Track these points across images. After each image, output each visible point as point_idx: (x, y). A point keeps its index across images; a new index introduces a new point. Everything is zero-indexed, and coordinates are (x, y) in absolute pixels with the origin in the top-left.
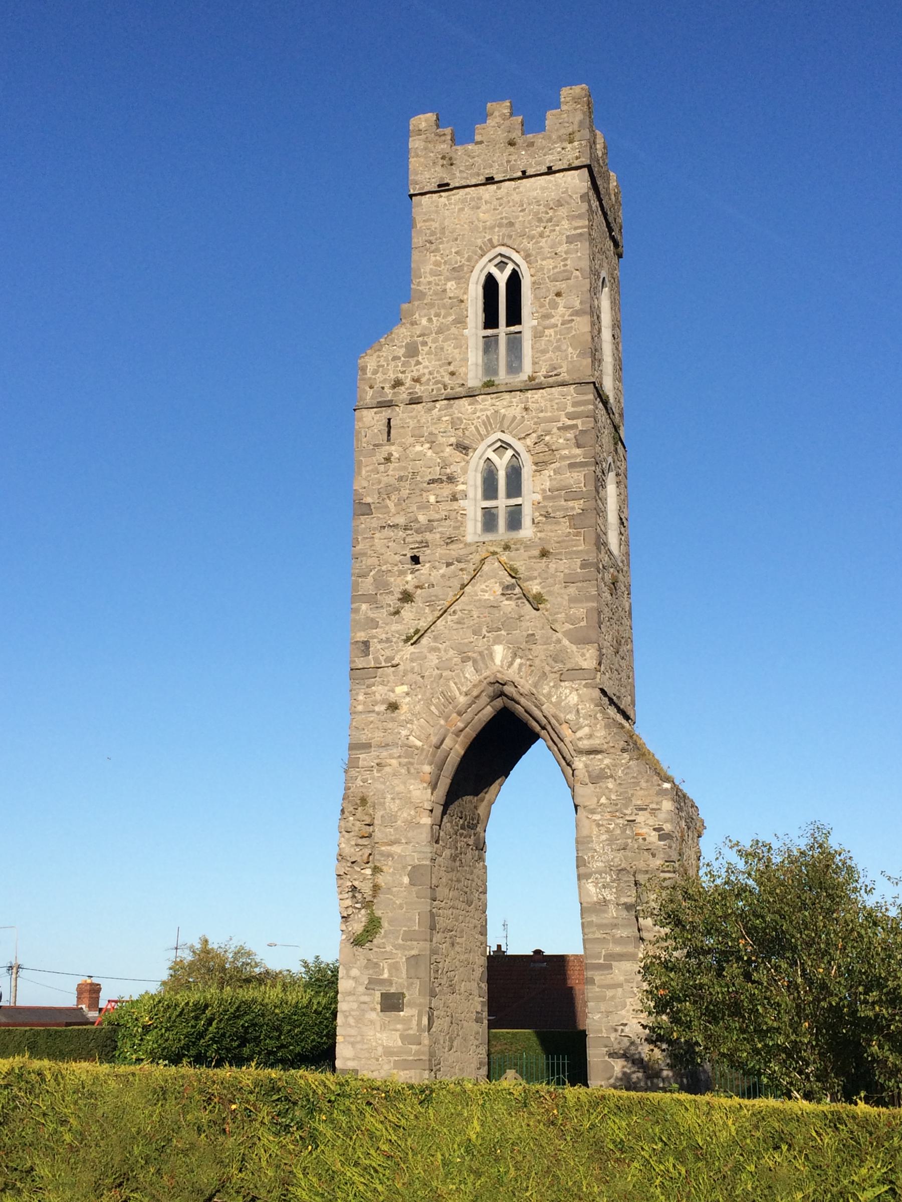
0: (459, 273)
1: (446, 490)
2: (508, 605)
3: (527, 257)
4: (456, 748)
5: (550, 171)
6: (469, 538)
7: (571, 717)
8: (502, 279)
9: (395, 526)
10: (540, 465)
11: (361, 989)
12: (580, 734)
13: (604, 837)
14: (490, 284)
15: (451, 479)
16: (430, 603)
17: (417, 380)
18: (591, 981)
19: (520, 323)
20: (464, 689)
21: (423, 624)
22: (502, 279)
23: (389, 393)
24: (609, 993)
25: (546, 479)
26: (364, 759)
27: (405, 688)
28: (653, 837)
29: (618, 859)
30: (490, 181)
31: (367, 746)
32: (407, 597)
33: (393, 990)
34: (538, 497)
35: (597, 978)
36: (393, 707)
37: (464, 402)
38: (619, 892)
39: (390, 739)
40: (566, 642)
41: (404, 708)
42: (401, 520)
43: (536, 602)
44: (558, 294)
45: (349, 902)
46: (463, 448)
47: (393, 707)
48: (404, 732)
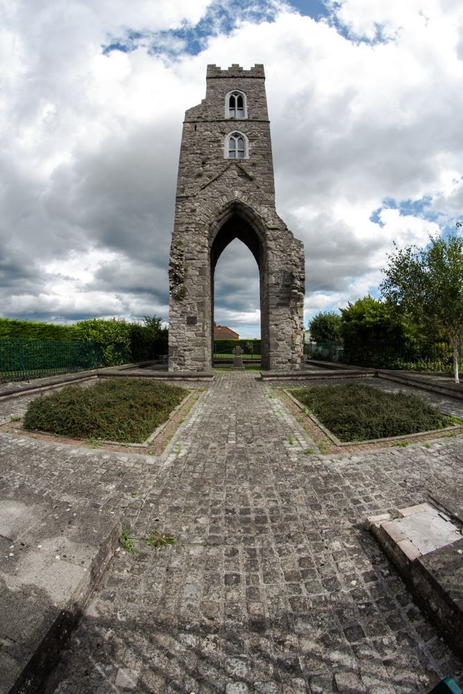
0: (224, 95)
1: (216, 145)
2: (241, 179)
3: (245, 93)
4: (217, 226)
5: (252, 77)
6: (225, 158)
7: (265, 216)
8: (236, 98)
9: (197, 153)
10: (251, 141)
11: (179, 315)
12: (269, 222)
13: (279, 259)
14: (232, 100)
15: (219, 141)
16: (210, 177)
17: (207, 116)
18: (272, 314)
19: (242, 106)
20: (223, 204)
21: (206, 183)
22: (236, 98)
23: (195, 119)
24: (278, 318)
25: (254, 144)
26: (182, 228)
27: (198, 204)
28: (298, 260)
29: (284, 267)
30: (233, 77)
31: (182, 224)
32: (199, 175)
33: (192, 316)
34: (250, 148)
35: (273, 313)
36: (193, 211)
37: (224, 123)
38: (284, 280)
39: (191, 221)
40: (263, 192)
41: (198, 210)
42: (199, 152)
43: (251, 179)
44: (256, 101)
45: (173, 282)
46: (224, 134)
47: (193, 211)
48: (198, 219)
